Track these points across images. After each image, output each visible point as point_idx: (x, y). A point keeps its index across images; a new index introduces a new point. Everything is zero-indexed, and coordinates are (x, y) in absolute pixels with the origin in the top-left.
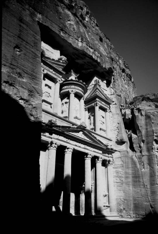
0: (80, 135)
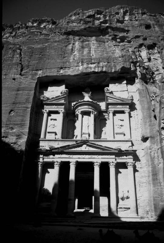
0: (84, 148)
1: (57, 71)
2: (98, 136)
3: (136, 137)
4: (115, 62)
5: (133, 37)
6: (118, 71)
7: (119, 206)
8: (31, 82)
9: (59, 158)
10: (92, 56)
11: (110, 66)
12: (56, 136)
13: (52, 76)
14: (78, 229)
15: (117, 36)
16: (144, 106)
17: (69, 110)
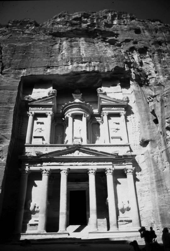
0: (77, 154)
1: (43, 70)
2: (90, 141)
3: (134, 141)
4: (107, 62)
5: (123, 41)
6: (112, 71)
7: (119, 218)
8: (14, 81)
9: (48, 165)
10: (82, 56)
11: (102, 66)
12: (44, 141)
13: (37, 75)
14: (81, 246)
15: (106, 39)
16: (141, 108)
17: (57, 113)
